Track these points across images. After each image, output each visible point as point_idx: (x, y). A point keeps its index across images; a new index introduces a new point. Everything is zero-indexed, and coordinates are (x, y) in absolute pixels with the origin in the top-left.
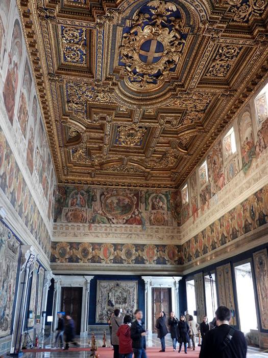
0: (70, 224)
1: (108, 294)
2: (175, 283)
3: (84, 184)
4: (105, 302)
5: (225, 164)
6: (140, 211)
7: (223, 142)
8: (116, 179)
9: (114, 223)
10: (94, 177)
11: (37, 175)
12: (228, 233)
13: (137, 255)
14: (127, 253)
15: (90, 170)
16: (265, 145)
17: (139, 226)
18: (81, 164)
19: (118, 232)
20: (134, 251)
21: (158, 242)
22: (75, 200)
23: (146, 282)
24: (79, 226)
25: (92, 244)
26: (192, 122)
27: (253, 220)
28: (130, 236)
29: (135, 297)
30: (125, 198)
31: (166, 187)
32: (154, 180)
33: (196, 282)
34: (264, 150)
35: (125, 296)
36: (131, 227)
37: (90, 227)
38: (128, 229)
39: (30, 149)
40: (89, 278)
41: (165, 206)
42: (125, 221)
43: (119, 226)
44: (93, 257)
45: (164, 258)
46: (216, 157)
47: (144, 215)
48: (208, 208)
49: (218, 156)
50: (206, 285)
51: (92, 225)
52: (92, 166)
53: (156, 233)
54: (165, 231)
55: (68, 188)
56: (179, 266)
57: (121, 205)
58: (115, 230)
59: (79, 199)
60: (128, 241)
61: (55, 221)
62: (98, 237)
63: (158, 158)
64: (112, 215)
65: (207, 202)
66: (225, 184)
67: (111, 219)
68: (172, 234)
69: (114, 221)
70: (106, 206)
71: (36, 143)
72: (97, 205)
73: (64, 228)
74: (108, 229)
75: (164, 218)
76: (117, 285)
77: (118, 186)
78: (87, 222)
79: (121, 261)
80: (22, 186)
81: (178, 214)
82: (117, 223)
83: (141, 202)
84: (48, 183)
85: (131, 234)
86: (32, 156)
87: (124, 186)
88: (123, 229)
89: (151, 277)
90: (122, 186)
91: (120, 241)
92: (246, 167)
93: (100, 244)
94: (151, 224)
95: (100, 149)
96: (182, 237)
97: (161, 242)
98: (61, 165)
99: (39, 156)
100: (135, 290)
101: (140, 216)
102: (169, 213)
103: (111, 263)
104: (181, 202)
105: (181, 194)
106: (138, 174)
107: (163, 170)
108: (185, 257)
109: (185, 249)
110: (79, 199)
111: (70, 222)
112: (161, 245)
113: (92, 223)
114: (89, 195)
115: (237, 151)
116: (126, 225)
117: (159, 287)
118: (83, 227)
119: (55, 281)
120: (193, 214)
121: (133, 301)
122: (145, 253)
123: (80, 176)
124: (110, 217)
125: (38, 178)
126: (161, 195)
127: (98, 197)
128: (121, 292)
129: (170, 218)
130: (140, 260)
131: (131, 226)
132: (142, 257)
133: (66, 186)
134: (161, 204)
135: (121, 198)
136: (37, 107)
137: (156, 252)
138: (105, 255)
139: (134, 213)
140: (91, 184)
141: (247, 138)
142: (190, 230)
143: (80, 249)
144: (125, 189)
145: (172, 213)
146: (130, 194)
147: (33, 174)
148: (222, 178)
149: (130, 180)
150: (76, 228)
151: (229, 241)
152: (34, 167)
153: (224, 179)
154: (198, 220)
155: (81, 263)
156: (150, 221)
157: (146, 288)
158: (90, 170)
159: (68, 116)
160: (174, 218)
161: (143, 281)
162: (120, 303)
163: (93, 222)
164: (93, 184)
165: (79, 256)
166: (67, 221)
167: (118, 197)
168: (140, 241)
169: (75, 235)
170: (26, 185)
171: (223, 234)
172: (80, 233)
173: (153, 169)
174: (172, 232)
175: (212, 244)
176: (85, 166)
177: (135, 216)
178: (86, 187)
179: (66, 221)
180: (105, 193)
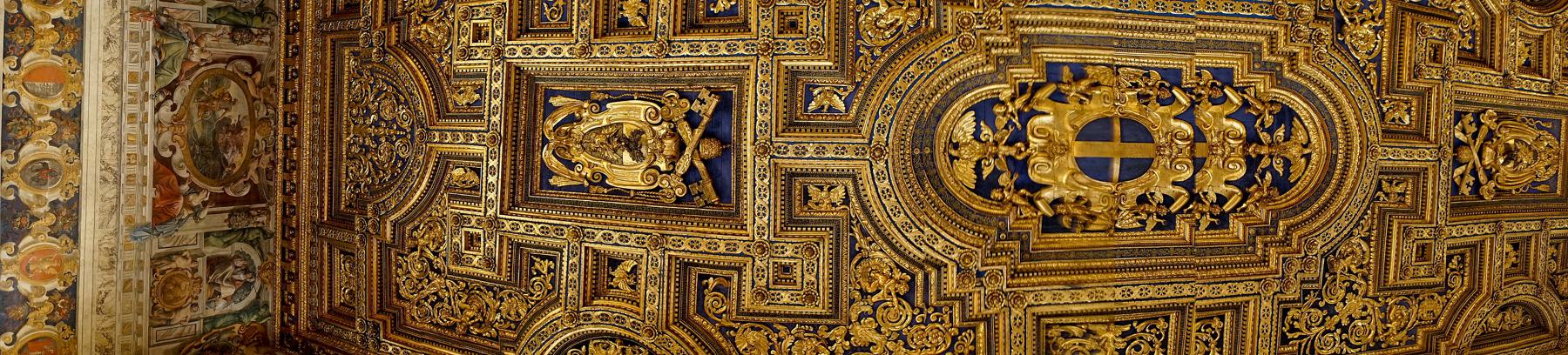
6: (203, 214)
9: (157, 109)
13: (37, 211)
17: (147, 213)
19: (127, 128)
20: (51, 195)
21: (86, 294)
28: (110, 177)
30: (244, 152)
36: (145, 178)
38: (135, 169)
41: (220, 306)
42: (167, 154)
44: (29, 24)
45: (25, 321)
47: (190, 231)
51: (150, 24)
53: (120, 287)
54: (130, 318)
57: (221, 138)
58: (132, 116)
62: (106, 47)
64: (186, 102)
69: (165, 112)
70: (217, 81)
72: (218, 44)
74: (135, 87)
82: (158, 123)
83: (231, 213)
88: (134, 149)
93: (78, 52)
94: (156, 260)
97: (88, 307)
102: (199, 325)
113: (157, 22)
114: (251, 15)
116: (151, 161)
122: (45, 241)
124: (178, 96)
126: (258, 284)
127: (245, 49)
129: (179, 331)
132: (29, 231)
134: (228, 291)
135: (246, 137)
137: (49, 286)
138: (37, 72)
139: (195, 189)
144: (275, 149)
145: (196, 338)
156: (169, 257)
163: (161, 28)
167: (247, 125)
177: (186, 196)
180: (258, 76)
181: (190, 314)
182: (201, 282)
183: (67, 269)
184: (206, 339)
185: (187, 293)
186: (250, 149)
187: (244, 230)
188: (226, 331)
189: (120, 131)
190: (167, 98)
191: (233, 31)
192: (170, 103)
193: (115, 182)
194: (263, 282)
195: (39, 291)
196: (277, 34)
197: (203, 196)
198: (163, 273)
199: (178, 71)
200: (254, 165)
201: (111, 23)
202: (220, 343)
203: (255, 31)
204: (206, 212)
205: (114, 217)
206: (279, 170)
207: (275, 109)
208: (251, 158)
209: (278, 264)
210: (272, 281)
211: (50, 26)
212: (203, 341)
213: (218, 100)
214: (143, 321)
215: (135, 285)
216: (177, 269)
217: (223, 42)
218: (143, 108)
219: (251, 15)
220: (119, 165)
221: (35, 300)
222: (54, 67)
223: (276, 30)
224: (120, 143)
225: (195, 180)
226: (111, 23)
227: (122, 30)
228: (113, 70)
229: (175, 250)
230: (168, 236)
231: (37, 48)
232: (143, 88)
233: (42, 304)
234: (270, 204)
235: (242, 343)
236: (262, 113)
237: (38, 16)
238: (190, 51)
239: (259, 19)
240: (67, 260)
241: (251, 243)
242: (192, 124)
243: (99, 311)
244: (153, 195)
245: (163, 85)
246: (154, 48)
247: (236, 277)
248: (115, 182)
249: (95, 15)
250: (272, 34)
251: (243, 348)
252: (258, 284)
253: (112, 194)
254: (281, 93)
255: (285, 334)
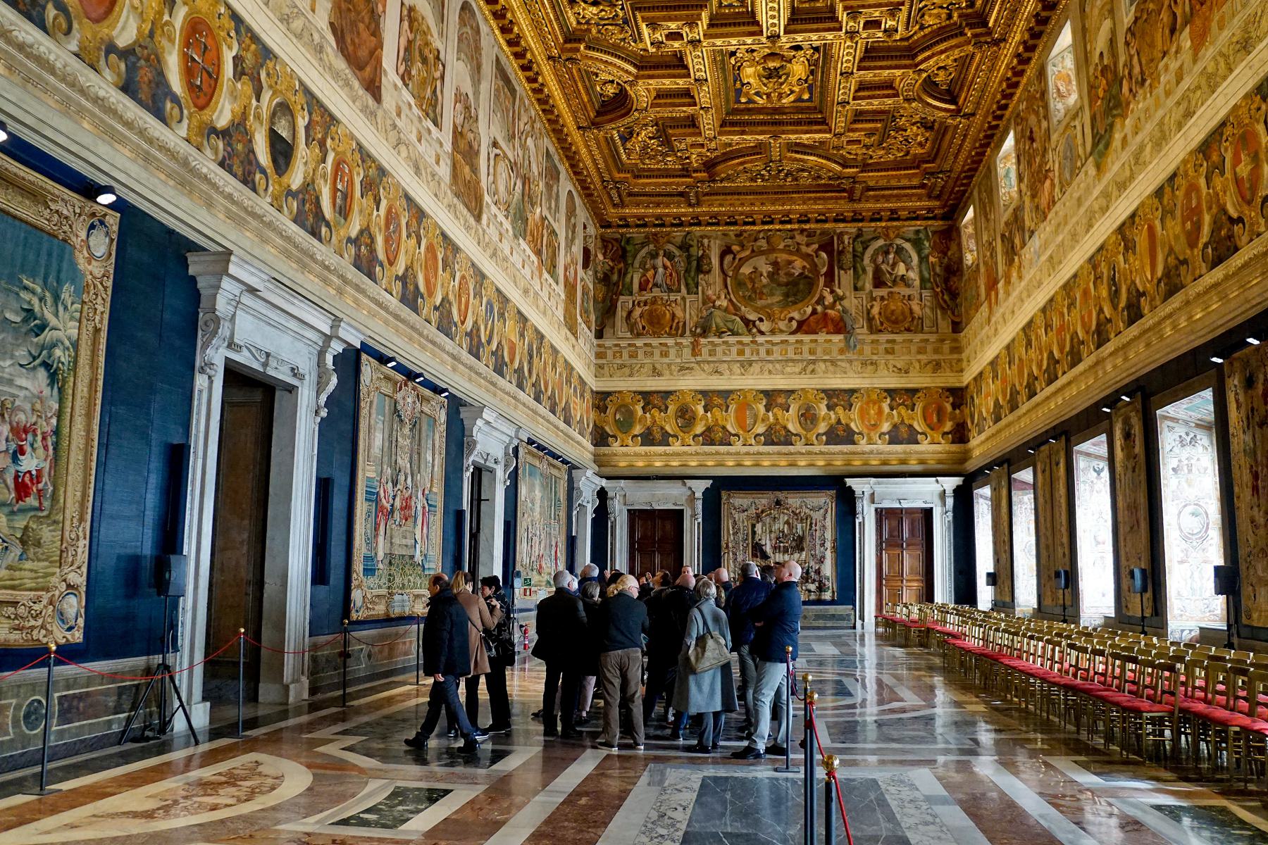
0: (639, 343)
1: (753, 526)
2: (943, 495)
3: (673, 225)
4: (745, 548)
5: (1054, 137)
6: (840, 292)
7: (1050, 70)
8: (762, 204)
9: (762, 333)
10: (698, 204)
11: (501, 218)
12: (1061, 350)
13: (833, 421)
14: (802, 415)
15: (680, 184)
16: (1142, 73)
17: (837, 338)
18: (652, 170)
19: (776, 356)
21: (894, 382)
22: (650, 274)
23: (858, 493)
24: (666, 345)
25: (704, 393)
26: (950, 17)
27: (1115, 307)
28: (811, 367)
29: (829, 535)
30: (795, 258)
31: (917, 218)
32: (877, 199)
33: (994, 490)
34: (1140, 92)
35: (801, 533)
36: (812, 341)
37: (695, 350)
38: (805, 349)
39: (465, 150)
40: (700, 487)
41: (913, 275)
42: (794, 324)
43: (777, 339)
44: (709, 429)
45: (911, 426)
46: (1033, 119)
47: (852, 303)
48: (1020, 278)
49: (1037, 113)
50: (1014, 499)
51: (703, 341)
52: (686, 172)
53: (890, 357)
54: (914, 349)
55: (628, 241)
56: (955, 447)
57: (783, 279)
58: (768, 352)
59: (661, 270)
60: (805, 381)
61: (599, 335)
62: (721, 374)
63: (870, 134)
64: (756, 310)
65: (1016, 258)
66: (1054, 203)
67: (754, 322)
68: (936, 357)
69: (764, 326)
70: (740, 284)
71: (488, 129)
72: (712, 284)
73: (625, 355)
74: (747, 351)
75: (911, 310)
76: (778, 503)
77: (771, 222)
78: (688, 333)
79: (785, 438)
80: (440, 257)
81: (954, 295)
82: (773, 332)
83: (841, 268)
84: (553, 233)
85: (814, 362)
86: (475, 170)
87: (790, 222)
88: (791, 349)
89: (873, 480)
90: (782, 222)
91: (782, 381)
92: (1101, 147)
93: (726, 394)
94: (873, 330)
95: (692, 123)
96: (965, 363)
97: (903, 380)
98: (596, 179)
99: (502, 167)
100: (828, 519)
101: (839, 307)
102: (926, 293)
103: (758, 443)
104: (961, 259)
105: (959, 236)
106: (825, 185)
107: (897, 166)
108: (973, 423)
109: (972, 398)
110: (661, 270)
111: (639, 335)
112: (901, 389)
114: (689, 257)
115: (1081, 97)
116: (799, 337)
117: (897, 505)
118: (677, 349)
119: (611, 494)
120: (988, 295)
121: (823, 545)
123: (658, 205)
124: (752, 316)
125: (507, 225)
126: (899, 241)
127: (715, 261)
128: (787, 522)
129: (928, 310)
130: (840, 435)
131: (813, 337)
132: (848, 425)
133: (622, 235)
134: (901, 269)
135: (782, 257)
136: (478, 32)
137: (886, 409)
139: (821, 300)
140: (691, 225)
141: (1101, 54)
142: (982, 343)
143: (672, 408)
144: (791, 230)
145: (936, 295)
146: (808, 245)
147: (484, 217)
148: (1048, 183)
149: (804, 203)
150: (657, 352)
151: (1064, 373)
152: (487, 198)
153: (1053, 185)
154: (999, 312)
155: (676, 447)
156: (870, 320)
157: (859, 509)
158: (680, 184)
159: (579, 41)
160: (942, 308)
161: (851, 492)
162: (786, 551)
163: (705, 332)
164: (699, 224)
165: (668, 428)
166: (632, 332)
167: (773, 256)
168: (839, 381)
169: (656, 372)
170: (456, 249)
171: (1051, 353)
172: (669, 365)
173: (866, 167)
174: (936, 351)
175: (1028, 383)
176: (667, 174)
177: (826, 308)
178: (678, 234)
179: (629, 335)
180: (735, 248)
181: (917, 301)
182: (891, 293)
183: (874, 397)
184: (938, 286)
185: (900, 304)
186: (791, 253)
187: (854, 256)
188: (934, 270)
189: (778, 361)
190: (754, 325)
191: (702, 272)
192: (757, 323)
193: (814, 364)
194: (897, 236)
195: (890, 416)
196: (701, 233)
197: (826, 293)
198: (882, 324)
199: (734, 317)
200: (804, 249)
201: (704, 370)
202: (942, 273)
203: (701, 253)
204: (838, 290)
205: (839, 363)
206: (807, 226)
207: (760, 231)
208: (798, 252)
209: (884, 224)
210: (897, 228)
211: (709, 414)
212: (939, 290)
213: (754, 283)
214: (918, 337)
215: (889, 346)
216: (880, 313)
217: (711, 281)
218: (762, 344)
219: (689, 257)
220: (802, 361)
221: (896, 419)
222: (736, 411)
223: (698, 234)
224: (787, 361)
225: (815, 299)
226: (704, 370)
227: (708, 362)
228: (736, 368)
229: (865, 315)
230: (854, 320)
231: (724, 423)
232: (748, 345)
233: (899, 414)
234: (835, 233)
235: (945, 254)
236: (763, 243)
237: (703, 422)
238: (719, 308)
239: (691, 249)
240: (869, 396)
241: (865, 249)
242: (773, 304)
243: (906, 372)
244: (824, 334)
245: (745, 329)
246: (719, 337)
247: (891, 262)
248: (814, 364)
249: (699, 382)
250: (702, 237)
251: (949, 253)
252: (899, 241)
253: (822, 365)
254: (748, 227)
255: (944, 217)
